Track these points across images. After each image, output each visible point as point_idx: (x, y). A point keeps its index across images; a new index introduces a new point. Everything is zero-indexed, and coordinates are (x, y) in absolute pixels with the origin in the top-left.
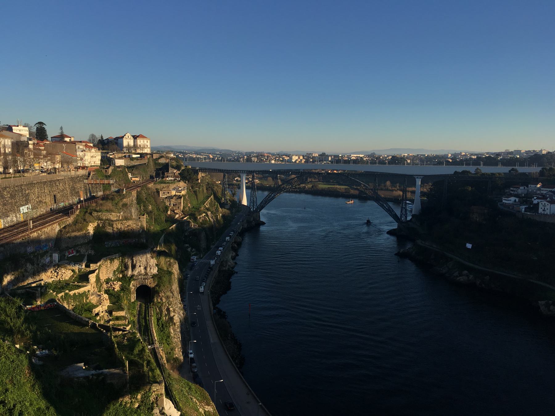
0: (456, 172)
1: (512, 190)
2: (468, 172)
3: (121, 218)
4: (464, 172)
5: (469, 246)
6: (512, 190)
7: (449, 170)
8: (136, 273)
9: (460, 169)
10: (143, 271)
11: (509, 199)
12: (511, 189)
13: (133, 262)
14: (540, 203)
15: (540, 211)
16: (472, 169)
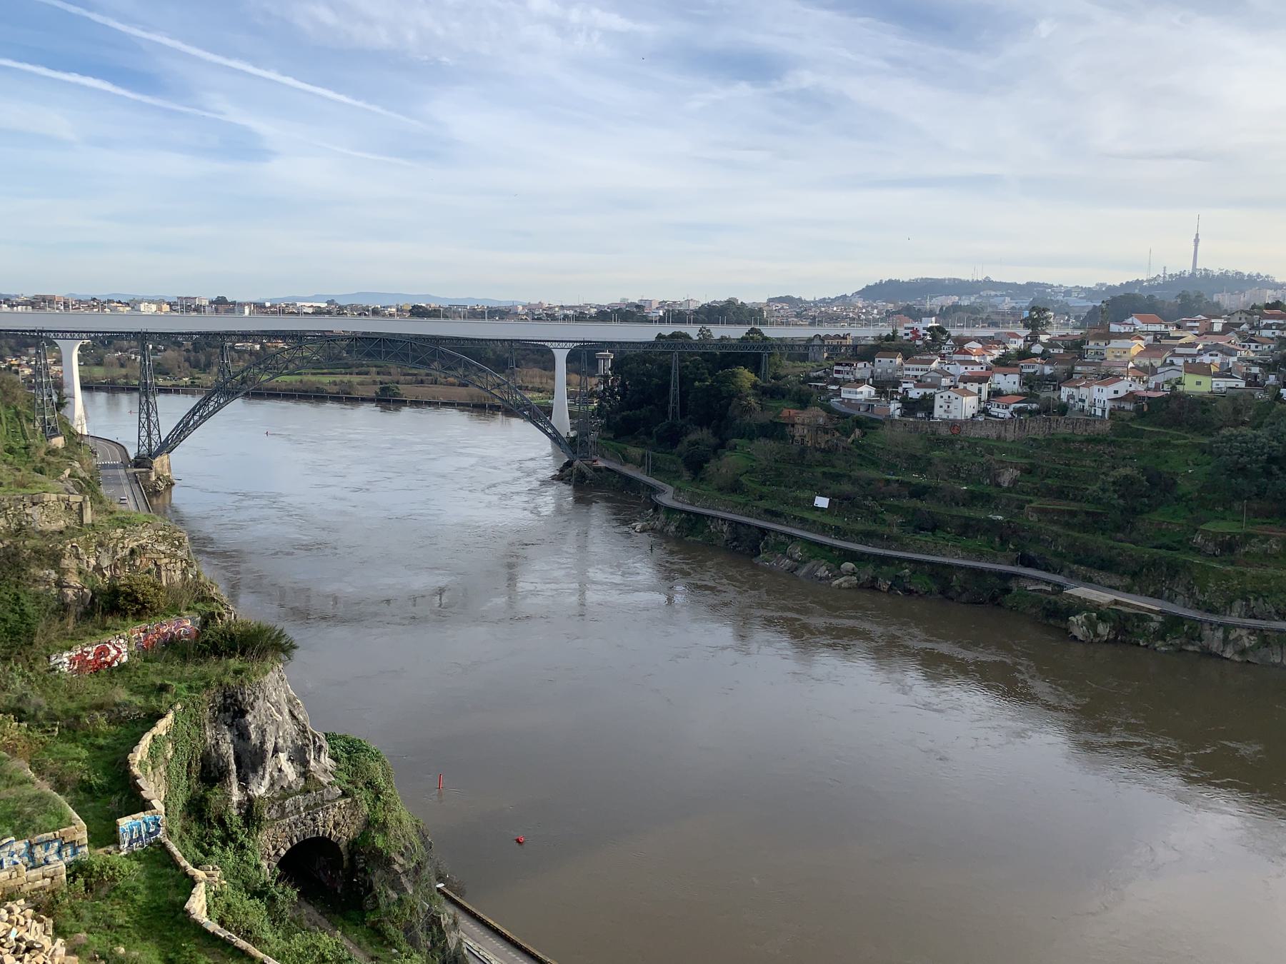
0: (660, 336)
1: (838, 372)
2: (687, 336)
3: (88, 518)
4: (674, 336)
5: (822, 502)
6: (838, 372)
7: (644, 333)
8: (260, 789)
9: (668, 329)
10: (290, 772)
11: (859, 390)
12: (836, 368)
13: (243, 735)
14: (937, 397)
15: (938, 412)
16: (693, 331)
